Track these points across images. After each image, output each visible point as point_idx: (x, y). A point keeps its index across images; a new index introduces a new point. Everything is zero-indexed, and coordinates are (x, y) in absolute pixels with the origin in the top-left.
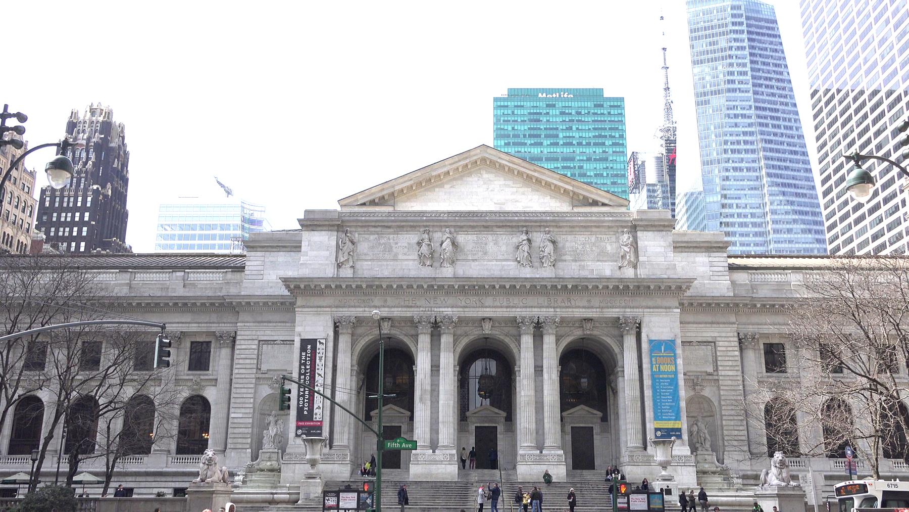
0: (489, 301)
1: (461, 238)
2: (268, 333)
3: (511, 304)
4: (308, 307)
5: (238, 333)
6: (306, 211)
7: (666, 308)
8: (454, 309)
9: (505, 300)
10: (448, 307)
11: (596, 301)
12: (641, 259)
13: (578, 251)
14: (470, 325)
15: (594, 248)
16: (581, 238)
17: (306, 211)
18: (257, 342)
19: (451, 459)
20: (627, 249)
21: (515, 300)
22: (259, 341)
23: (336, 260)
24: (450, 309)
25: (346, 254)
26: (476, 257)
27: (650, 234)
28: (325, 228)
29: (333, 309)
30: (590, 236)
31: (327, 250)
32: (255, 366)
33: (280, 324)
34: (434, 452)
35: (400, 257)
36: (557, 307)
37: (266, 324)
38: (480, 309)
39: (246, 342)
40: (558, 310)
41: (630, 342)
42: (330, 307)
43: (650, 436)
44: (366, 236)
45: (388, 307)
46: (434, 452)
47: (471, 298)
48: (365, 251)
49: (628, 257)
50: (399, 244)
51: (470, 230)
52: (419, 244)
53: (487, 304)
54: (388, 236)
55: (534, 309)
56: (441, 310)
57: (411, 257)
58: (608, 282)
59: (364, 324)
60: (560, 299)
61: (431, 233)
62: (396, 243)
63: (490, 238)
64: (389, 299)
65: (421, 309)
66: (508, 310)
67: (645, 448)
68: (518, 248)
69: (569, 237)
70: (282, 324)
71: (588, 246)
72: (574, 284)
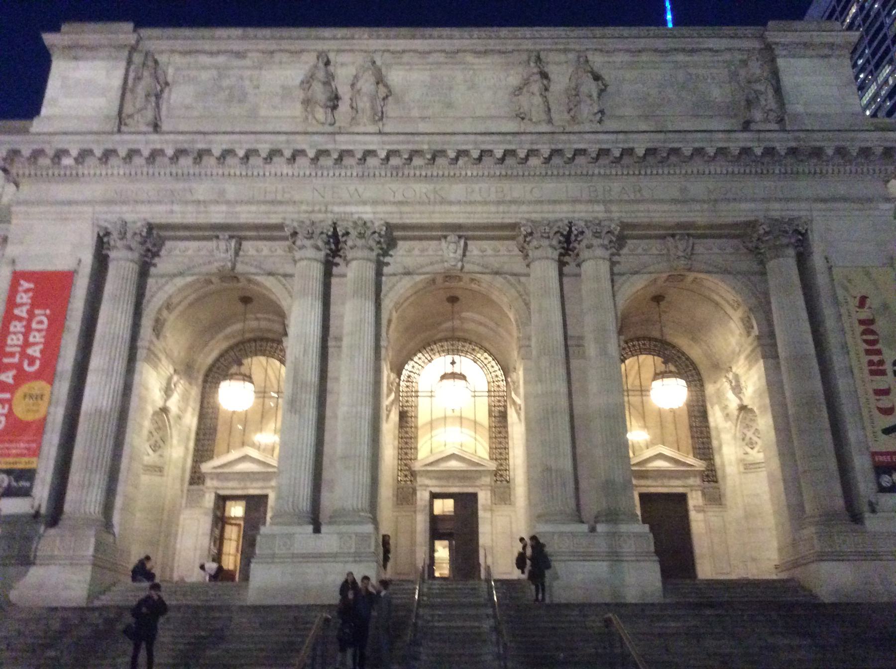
8: (380, 209)
12: (790, 108)
15: (684, 94)
24: (368, 208)
26: (429, 112)
27: (803, 63)
35: (263, 112)
36: (611, 201)
40: (614, 208)
43: (865, 485)
49: (763, 102)
50: (262, 89)
53: (453, 197)
55: (558, 208)
56: (349, 209)
58: (728, 140)
60: (616, 186)
62: (257, 87)
63: (459, 76)
66: (501, 208)
67: (856, 518)
72: (650, 145)
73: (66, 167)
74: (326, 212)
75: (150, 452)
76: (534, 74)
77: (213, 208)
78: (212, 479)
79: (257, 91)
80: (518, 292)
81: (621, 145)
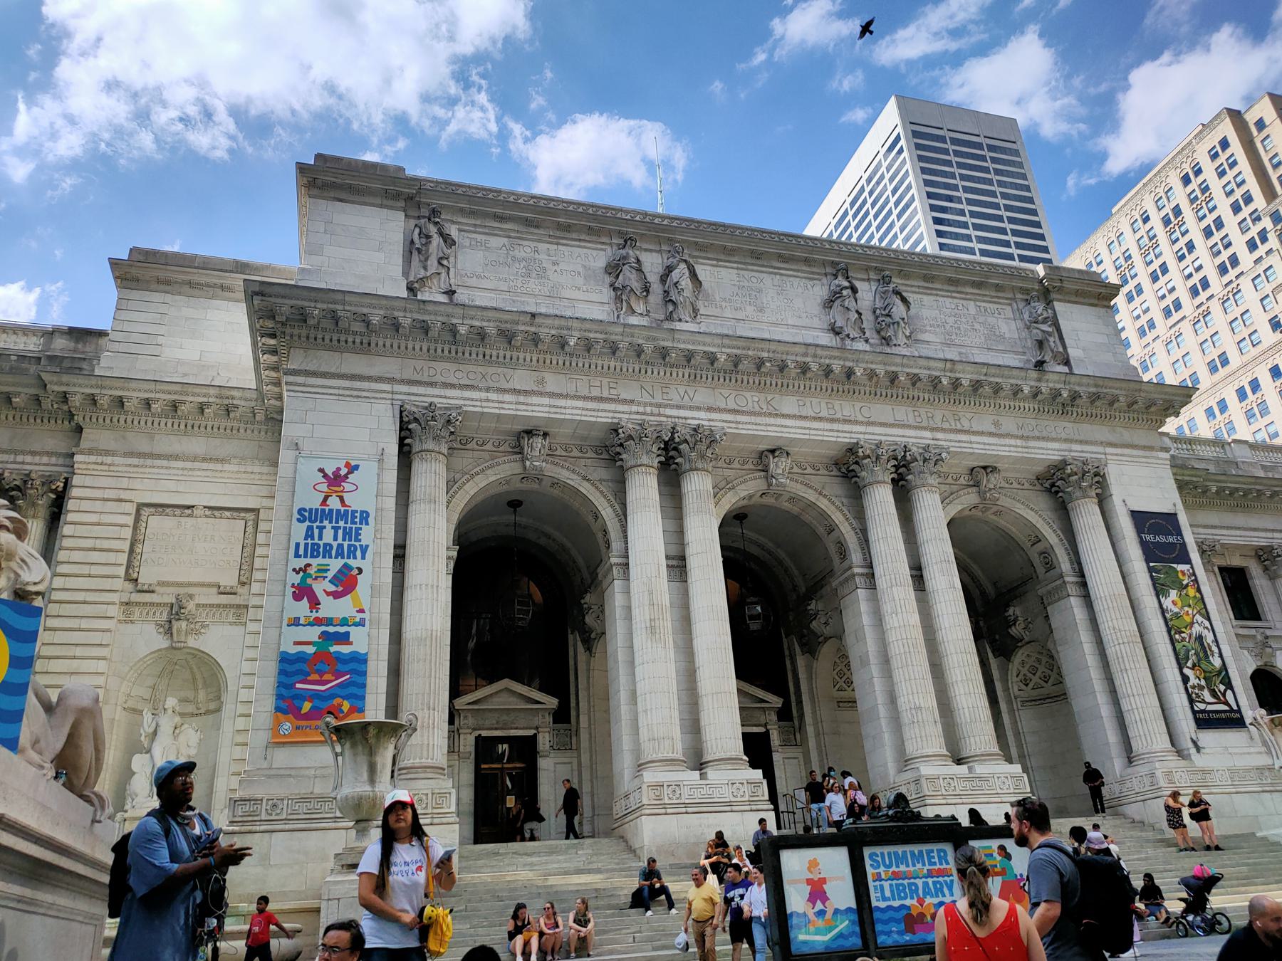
0: (789, 404)
1: (703, 271)
2: (171, 485)
3: (839, 416)
4: (324, 375)
5: (76, 480)
6: (319, 157)
7: (1145, 448)
9: (823, 405)
10: (698, 408)
11: (1009, 424)
13: (948, 327)
14: (735, 465)
15: (977, 326)
16: (948, 303)
17: (319, 157)
18: (131, 508)
19: (753, 794)
20: (1045, 327)
21: (845, 408)
22: (140, 506)
23: (405, 273)
24: (702, 414)
26: (740, 315)
28: (371, 200)
29: (398, 388)
30: (964, 302)
31: (380, 250)
32: (121, 571)
33: (205, 465)
34: (703, 776)
37: (165, 463)
38: (772, 420)
39: (98, 506)
40: (940, 435)
41: (1087, 517)
42: (391, 380)
44: (479, 237)
45: (552, 395)
46: (703, 776)
47: (748, 395)
48: (479, 270)
50: (563, 266)
51: (722, 257)
52: (614, 269)
53: (785, 412)
54: (532, 244)
56: (682, 413)
57: (595, 297)
59: (473, 445)
60: (938, 415)
62: (553, 264)
64: (549, 377)
65: (634, 408)
68: (829, 304)
69: (927, 299)
70: (212, 466)
71: (963, 320)
72: (976, 377)
73: (355, 333)
74: (659, 415)
76: (846, 288)
77: (535, 400)
78: (465, 717)
79: (556, 267)
80: (844, 515)
81: (949, 374)
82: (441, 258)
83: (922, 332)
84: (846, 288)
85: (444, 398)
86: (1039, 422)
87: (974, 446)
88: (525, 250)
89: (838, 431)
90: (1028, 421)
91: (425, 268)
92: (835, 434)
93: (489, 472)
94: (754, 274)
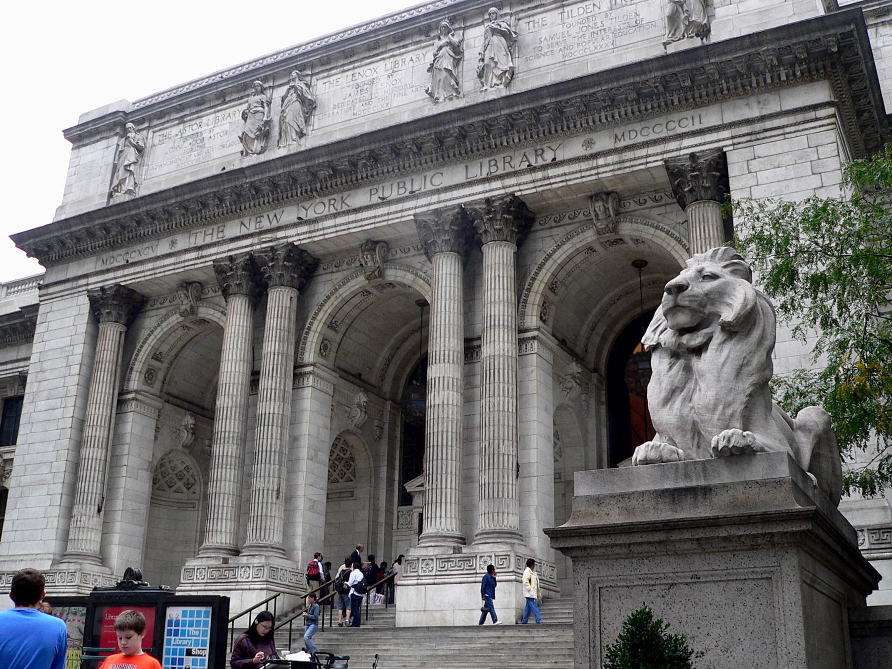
11: (604, 142)
13: (570, 40)
25: (122, 169)
55: (456, 193)
59: (158, 305)
61: (268, 92)
75: (185, 490)
76: (440, 48)
79: (212, 134)
82: (126, 166)
83: (538, 57)
84: (440, 48)
85: (110, 280)
86: (643, 124)
87: (552, 181)
88: (190, 129)
89: (402, 211)
90: (630, 127)
91: (117, 178)
92: (399, 215)
93: (164, 324)
94: (371, 66)
